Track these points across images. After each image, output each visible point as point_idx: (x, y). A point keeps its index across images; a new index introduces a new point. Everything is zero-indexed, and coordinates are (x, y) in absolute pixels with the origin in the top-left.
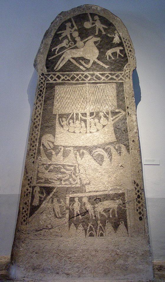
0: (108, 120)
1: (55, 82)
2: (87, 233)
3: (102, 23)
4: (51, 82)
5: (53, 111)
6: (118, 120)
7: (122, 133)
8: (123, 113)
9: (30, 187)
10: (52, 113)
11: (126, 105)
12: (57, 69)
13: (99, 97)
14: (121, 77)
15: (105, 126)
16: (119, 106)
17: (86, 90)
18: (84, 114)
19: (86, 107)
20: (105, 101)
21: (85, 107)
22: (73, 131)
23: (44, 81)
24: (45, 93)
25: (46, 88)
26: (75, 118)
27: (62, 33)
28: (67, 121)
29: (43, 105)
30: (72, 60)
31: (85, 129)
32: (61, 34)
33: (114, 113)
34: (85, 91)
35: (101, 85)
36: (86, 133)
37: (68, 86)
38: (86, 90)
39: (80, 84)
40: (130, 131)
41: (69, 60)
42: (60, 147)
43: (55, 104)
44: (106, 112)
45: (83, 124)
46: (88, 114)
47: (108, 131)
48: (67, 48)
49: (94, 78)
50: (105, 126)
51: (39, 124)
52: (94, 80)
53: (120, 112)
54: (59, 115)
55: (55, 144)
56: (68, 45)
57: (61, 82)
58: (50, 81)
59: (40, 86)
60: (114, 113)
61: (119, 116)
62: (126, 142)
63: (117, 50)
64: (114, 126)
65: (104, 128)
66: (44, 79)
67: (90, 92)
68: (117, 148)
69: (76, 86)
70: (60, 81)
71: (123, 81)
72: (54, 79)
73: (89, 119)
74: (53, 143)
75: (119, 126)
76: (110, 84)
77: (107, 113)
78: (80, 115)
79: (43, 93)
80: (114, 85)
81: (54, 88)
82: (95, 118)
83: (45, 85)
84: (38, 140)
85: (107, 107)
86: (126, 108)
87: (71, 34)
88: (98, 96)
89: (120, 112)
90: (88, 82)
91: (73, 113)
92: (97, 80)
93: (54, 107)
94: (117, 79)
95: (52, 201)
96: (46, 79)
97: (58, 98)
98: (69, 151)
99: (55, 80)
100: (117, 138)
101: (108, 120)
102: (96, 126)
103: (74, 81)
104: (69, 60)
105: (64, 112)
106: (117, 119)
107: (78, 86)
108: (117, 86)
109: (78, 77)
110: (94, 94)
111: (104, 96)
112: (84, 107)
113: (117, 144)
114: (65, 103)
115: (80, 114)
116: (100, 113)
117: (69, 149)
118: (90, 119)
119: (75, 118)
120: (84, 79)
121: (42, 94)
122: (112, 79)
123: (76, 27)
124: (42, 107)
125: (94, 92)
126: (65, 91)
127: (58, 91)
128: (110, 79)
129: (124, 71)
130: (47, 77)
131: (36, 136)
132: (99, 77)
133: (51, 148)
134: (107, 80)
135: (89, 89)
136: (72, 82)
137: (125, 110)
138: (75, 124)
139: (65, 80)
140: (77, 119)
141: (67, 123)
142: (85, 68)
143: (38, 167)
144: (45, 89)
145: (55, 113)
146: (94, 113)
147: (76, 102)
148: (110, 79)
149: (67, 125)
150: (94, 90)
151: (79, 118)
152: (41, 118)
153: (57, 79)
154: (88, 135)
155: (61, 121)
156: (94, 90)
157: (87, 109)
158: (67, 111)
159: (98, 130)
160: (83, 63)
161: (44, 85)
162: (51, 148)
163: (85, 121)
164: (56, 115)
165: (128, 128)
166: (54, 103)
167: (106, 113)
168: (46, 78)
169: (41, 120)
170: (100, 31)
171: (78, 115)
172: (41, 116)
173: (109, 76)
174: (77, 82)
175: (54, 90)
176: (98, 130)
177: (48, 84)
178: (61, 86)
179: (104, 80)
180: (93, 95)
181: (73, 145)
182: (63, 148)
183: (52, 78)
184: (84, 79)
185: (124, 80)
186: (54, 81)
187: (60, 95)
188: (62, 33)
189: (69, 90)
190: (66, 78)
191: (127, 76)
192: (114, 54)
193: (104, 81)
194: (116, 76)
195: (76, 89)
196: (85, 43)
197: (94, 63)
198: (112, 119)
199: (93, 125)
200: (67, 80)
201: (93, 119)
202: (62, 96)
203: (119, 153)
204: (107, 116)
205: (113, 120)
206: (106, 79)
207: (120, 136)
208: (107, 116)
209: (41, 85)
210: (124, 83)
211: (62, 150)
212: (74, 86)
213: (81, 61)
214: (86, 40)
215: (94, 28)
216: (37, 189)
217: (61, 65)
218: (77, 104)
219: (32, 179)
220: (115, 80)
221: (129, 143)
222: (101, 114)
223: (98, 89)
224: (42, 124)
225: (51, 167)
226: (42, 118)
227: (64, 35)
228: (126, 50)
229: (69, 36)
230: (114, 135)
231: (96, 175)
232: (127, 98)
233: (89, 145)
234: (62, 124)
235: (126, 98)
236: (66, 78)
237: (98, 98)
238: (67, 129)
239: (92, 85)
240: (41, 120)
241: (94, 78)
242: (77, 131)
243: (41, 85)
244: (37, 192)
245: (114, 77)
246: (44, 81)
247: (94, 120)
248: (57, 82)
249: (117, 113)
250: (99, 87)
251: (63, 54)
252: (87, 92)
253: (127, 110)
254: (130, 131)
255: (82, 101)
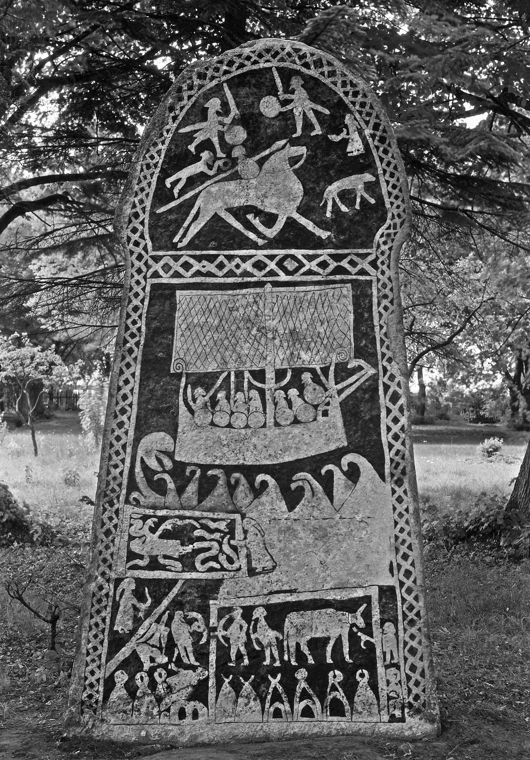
2: (267, 705)
3: (314, 99)
9: (108, 581)
12: (180, 241)
16: (359, 353)
27: (196, 131)
30: (223, 215)
41: (216, 217)
53: (360, 368)
56: (215, 168)
58: (161, 277)
83: (148, 289)
84: (129, 450)
89: (360, 368)
95: (171, 618)
104: (216, 217)
115: (247, 375)
122: (339, 270)
129: (375, 246)
131: (123, 436)
140: (239, 388)
142: (264, 237)
143: (131, 525)
152: (137, 387)
160: (257, 222)
170: (308, 126)
183: (167, 268)
188: (196, 131)
196: (261, 163)
197: (291, 223)
202: (196, 321)
213: (250, 217)
214: (267, 152)
216: (128, 585)
217: (194, 230)
219: (115, 557)
228: (383, 185)
231: (291, 546)
244: (127, 594)
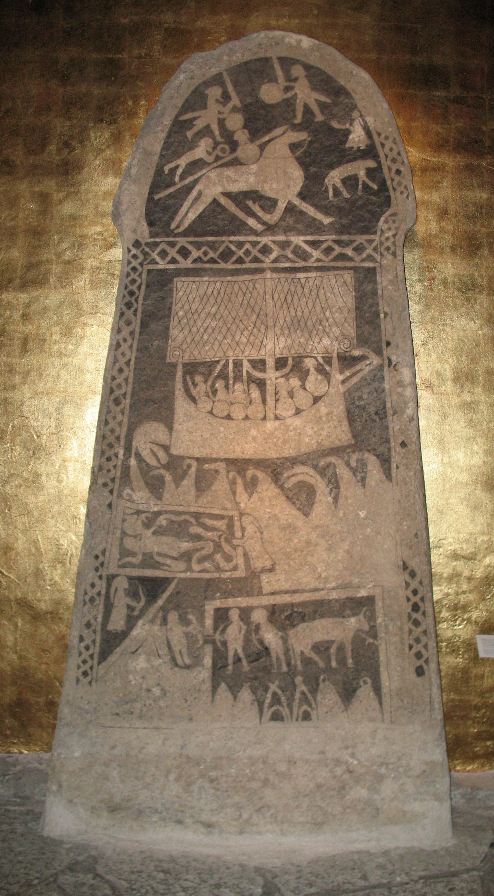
0: (329, 382)
1: (172, 266)
2: (265, 710)
3: (314, 88)
4: (160, 267)
5: (168, 354)
6: (360, 381)
7: (371, 419)
8: (375, 361)
10: (164, 358)
11: (383, 337)
12: (178, 227)
13: (303, 313)
14: (369, 251)
15: (320, 398)
16: (362, 340)
17: (265, 292)
18: (259, 364)
19: (264, 343)
20: (320, 324)
21: (262, 343)
22: (225, 413)
23: (141, 264)
24: (145, 299)
25: (148, 286)
26: (231, 374)
27: (195, 119)
28: (209, 383)
29: (137, 336)
30: (223, 201)
31: (261, 408)
32: (190, 123)
33: (347, 361)
34: (261, 292)
35: (310, 274)
36: (264, 418)
37: (212, 279)
38: (265, 292)
39: (247, 271)
40: (395, 413)
41: (215, 201)
42: (188, 461)
43: (174, 332)
44: (323, 357)
45: (255, 394)
46: (270, 363)
47: (328, 414)
48: (209, 164)
49: (290, 256)
50: (320, 398)
51: (125, 393)
52: (288, 260)
53: (363, 358)
54: (185, 365)
55: (174, 452)
57: (191, 266)
59: (130, 279)
60: (347, 361)
61: (361, 370)
62: (382, 449)
63: (360, 169)
64: (346, 400)
65: (317, 405)
66: (141, 257)
67: (276, 296)
68: (353, 464)
69: (235, 278)
70: (187, 264)
71: (376, 265)
72: (169, 258)
73: (274, 379)
74: (166, 448)
75: (360, 398)
76: (336, 272)
77: (327, 359)
78: (246, 366)
79: (137, 300)
80: (348, 277)
81: (171, 286)
82: (291, 375)
83: (144, 276)
85: (326, 342)
86: (384, 345)
87: (221, 123)
88: (299, 308)
89: (363, 358)
90: (271, 265)
91: (227, 361)
92: (299, 260)
93: (170, 341)
94: (358, 258)
96: (145, 259)
97: (181, 313)
98: (213, 472)
99: (173, 261)
100: (354, 437)
101: (329, 382)
102: (292, 398)
103: (229, 263)
105: (199, 357)
106: (355, 380)
107: (241, 278)
108: (357, 280)
109: (241, 253)
110: (289, 301)
111: (318, 308)
112: (257, 341)
113: (354, 452)
114: (202, 330)
115: (246, 364)
116: (307, 360)
117: (212, 466)
118: (276, 379)
119: (231, 374)
120: (260, 256)
121: (133, 301)
122: (342, 257)
123: (235, 101)
124: (136, 341)
125: (289, 298)
126: (201, 292)
127: (181, 294)
128: (336, 259)
129: (379, 233)
130: (150, 252)
131: (118, 429)
132: (305, 252)
133: (160, 463)
134: (327, 260)
135: (274, 287)
136: (222, 265)
137: (379, 352)
138: (231, 391)
139: (203, 262)
140: (238, 378)
141: (209, 389)
142: (264, 223)
143: (124, 520)
144: (143, 287)
145: (174, 360)
146: (287, 360)
147: (234, 328)
148: (336, 259)
149: (209, 397)
150: (289, 290)
151: (245, 373)
153: (179, 258)
154: (270, 425)
155: (190, 383)
156: (289, 290)
157: (268, 347)
158: (208, 354)
159: (298, 412)
160: (256, 208)
161: (140, 275)
162: (160, 463)
163: (261, 384)
164: (174, 366)
165: (389, 405)
166: (171, 329)
167: (325, 361)
168: (146, 254)
169: (131, 380)
170: (307, 110)
171: (241, 365)
172: (132, 367)
173: (333, 250)
174: (238, 266)
175: (171, 290)
176: (298, 412)
177: (152, 274)
178: (191, 279)
179: (318, 260)
180: (285, 306)
181: (227, 456)
182: (195, 464)
183: (163, 254)
184: (260, 256)
185: (379, 260)
186: (170, 262)
187: (187, 307)
188: (195, 119)
189: (215, 292)
190: (205, 254)
191: (388, 249)
192: (350, 181)
193: (320, 264)
194: (354, 249)
195: (236, 288)
196: (262, 147)
197: (290, 209)
198: (340, 378)
199: (284, 393)
200: (208, 262)
201: (282, 380)
202: (194, 307)
203: (359, 478)
204: (327, 368)
205: (343, 382)
206: (323, 258)
207: (363, 428)
208: (327, 368)
209: (133, 276)
210: (378, 270)
211: (193, 469)
212: (229, 278)
213: (250, 203)
214: (267, 138)
215: (289, 104)
216: (121, 584)
217: (192, 216)
218: (238, 333)
219: (107, 554)
220: (351, 259)
221: (389, 449)
222: (310, 363)
223: (299, 288)
224: (133, 394)
225: (162, 521)
226: (135, 375)
227: (200, 124)
228: (385, 170)
229: (215, 127)
230: (345, 426)
232: (386, 314)
233: (272, 454)
234: (194, 392)
235: (382, 316)
236: (205, 254)
237: (299, 314)
238: (209, 408)
239: (283, 275)
240: (131, 380)
241: (290, 256)
242: (238, 413)
243: (133, 276)
245: (349, 252)
246: (141, 264)
247: (288, 380)
248: (178, 266)
249: (353, 361)
250: (303, 281)
251: (196, 182)
252: (267, 297)
253: (385, 352)
254: (395, 413)
255: (252, 325)
